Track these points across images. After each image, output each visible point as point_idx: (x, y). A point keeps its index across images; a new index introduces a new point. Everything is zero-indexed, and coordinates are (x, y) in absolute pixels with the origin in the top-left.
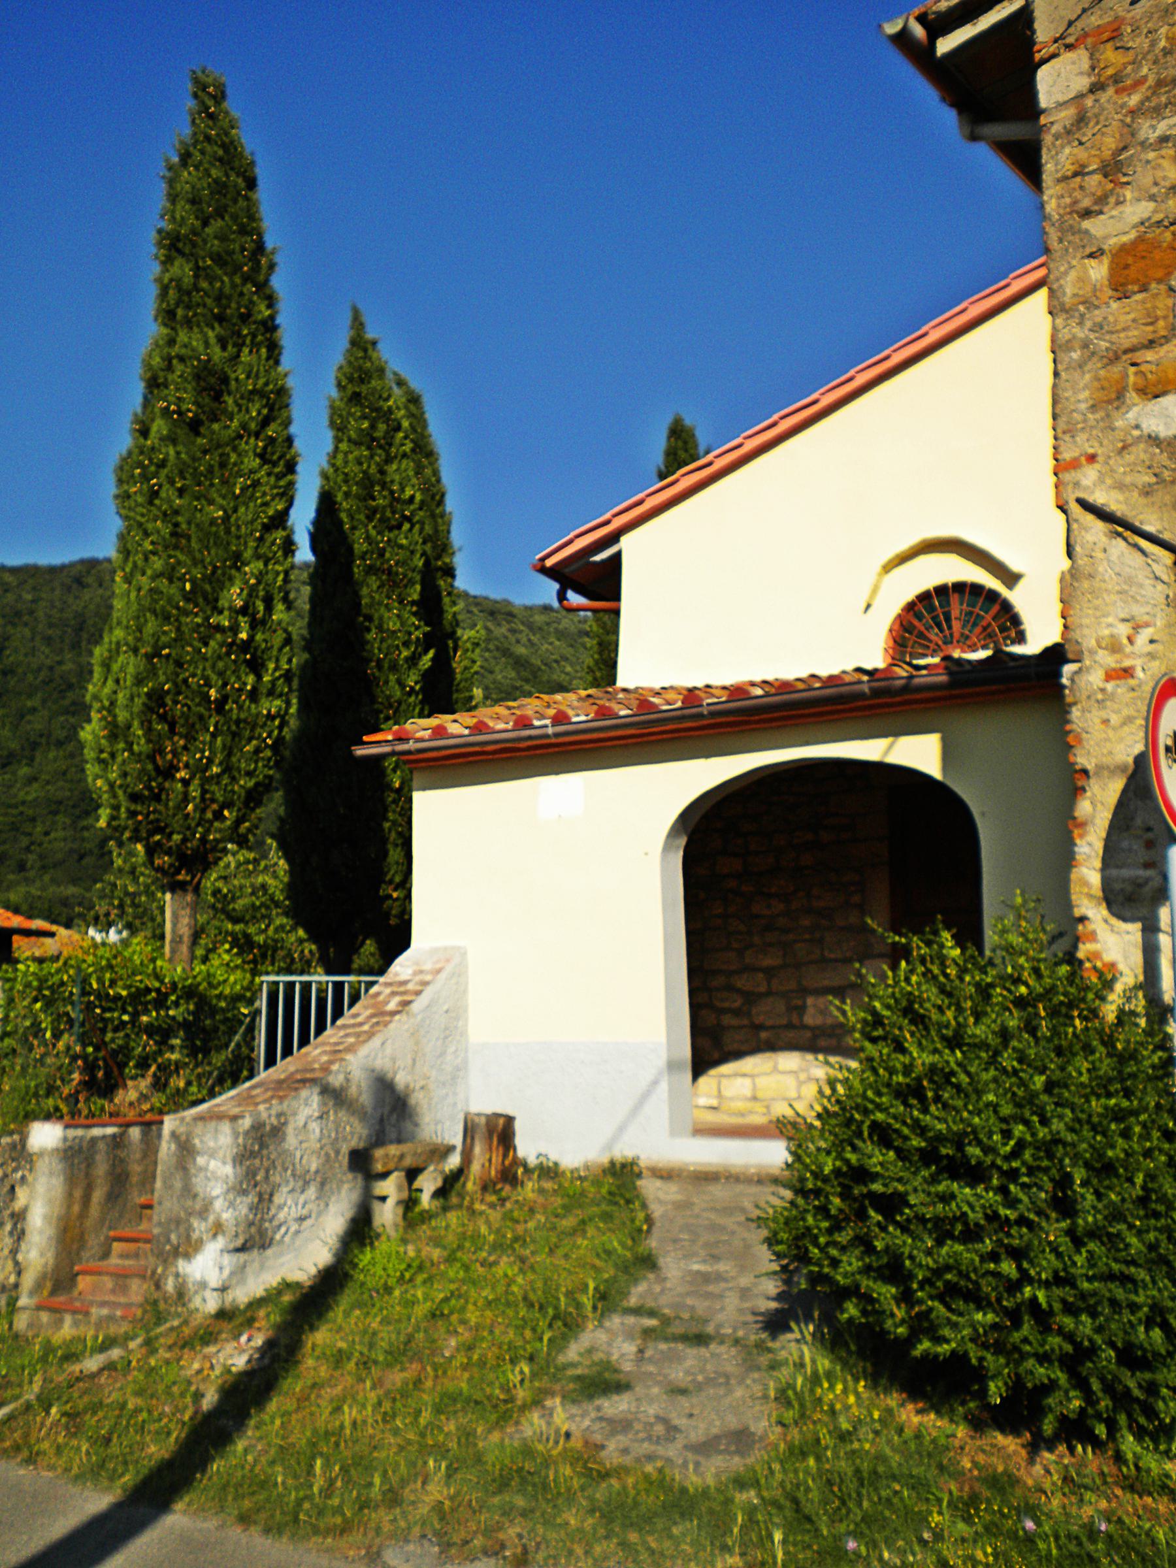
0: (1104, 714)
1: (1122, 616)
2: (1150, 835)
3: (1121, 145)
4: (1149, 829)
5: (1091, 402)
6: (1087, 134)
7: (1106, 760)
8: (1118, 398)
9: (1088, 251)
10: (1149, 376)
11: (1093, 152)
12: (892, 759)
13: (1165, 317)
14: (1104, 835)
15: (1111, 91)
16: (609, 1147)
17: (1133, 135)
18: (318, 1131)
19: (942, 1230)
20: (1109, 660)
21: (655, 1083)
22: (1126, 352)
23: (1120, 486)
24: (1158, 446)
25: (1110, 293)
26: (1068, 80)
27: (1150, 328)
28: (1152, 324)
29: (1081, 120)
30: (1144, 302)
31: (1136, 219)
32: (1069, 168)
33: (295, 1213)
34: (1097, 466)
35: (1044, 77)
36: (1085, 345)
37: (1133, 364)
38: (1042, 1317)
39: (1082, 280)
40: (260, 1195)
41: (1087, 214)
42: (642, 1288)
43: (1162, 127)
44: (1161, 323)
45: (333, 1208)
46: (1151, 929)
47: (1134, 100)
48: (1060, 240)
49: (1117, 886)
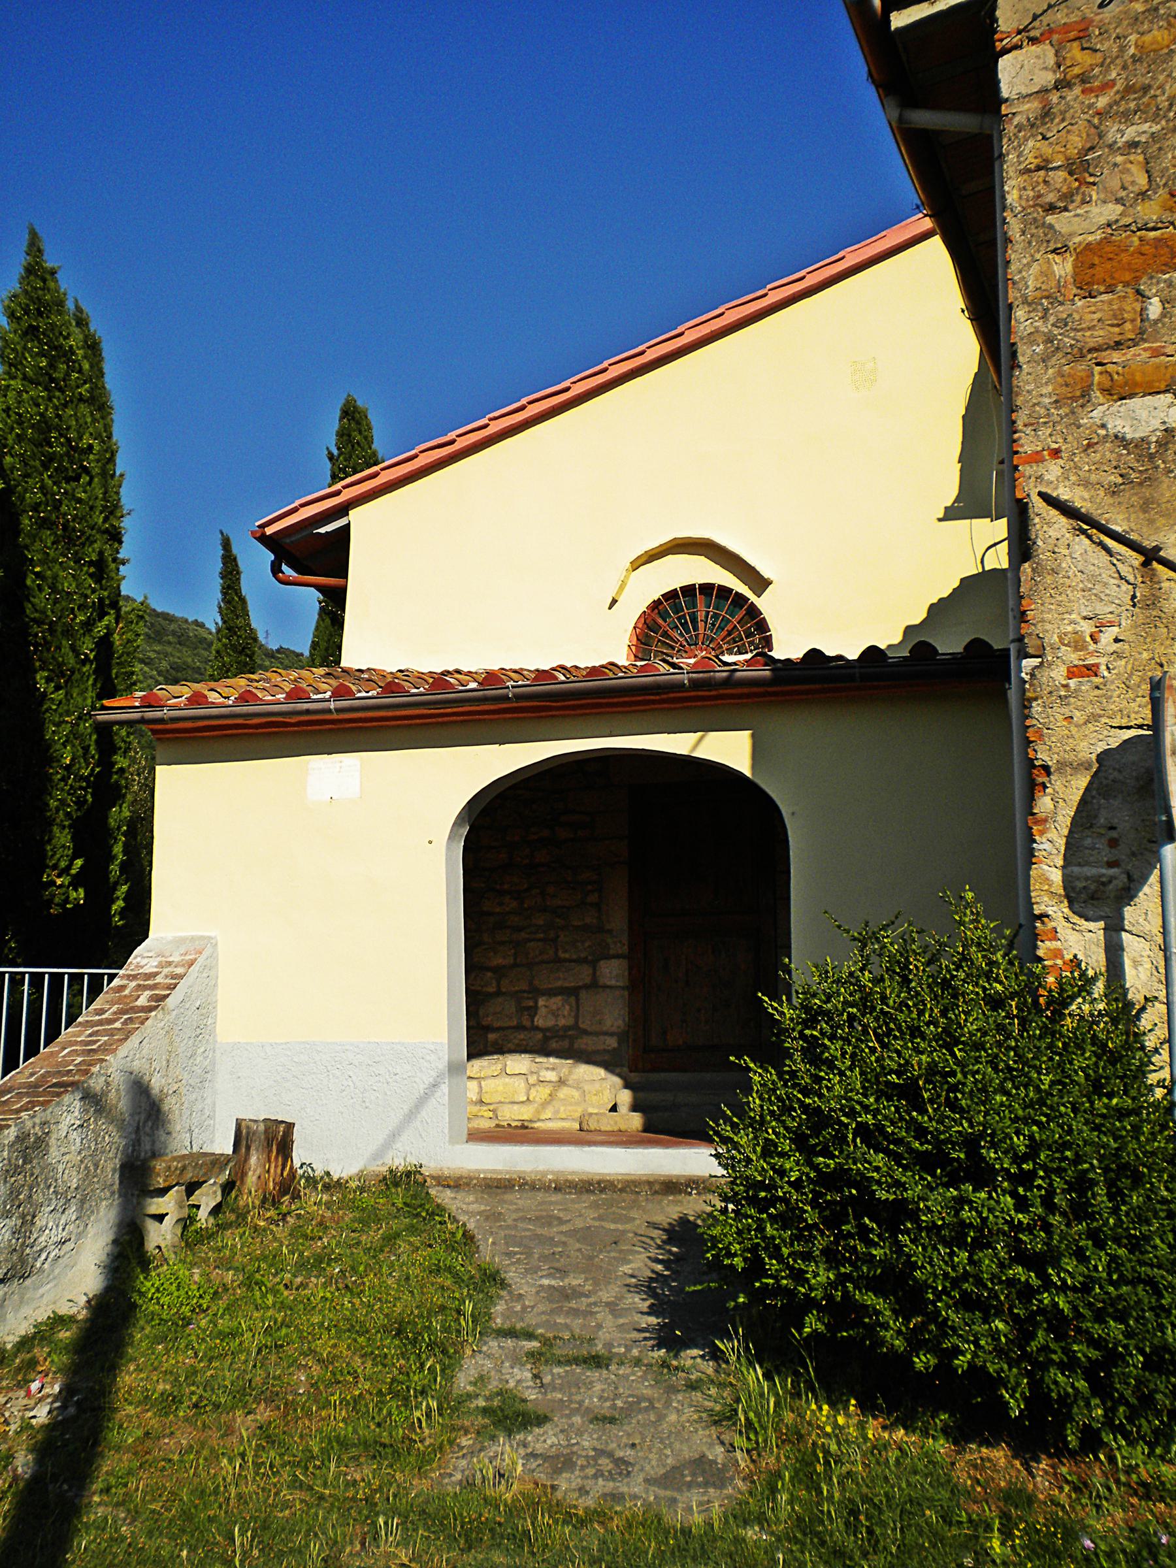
0: (1066, 711)
1: (1085, 614)
2: (1114, 834)
3: (1088, 145)
4: (1112, 828)
5: (1054, 398)
6: (1052, 131)
7: (1070, 757)
8: (1083, 396)
9: (1052, 246)
10: (1116, 377)
11: (1058, 148)
12: (701, 753)
13: (1133, 321)
14: (1066, 832)
15: (1077, 90)
16: (378, 1155)
17: (1100, 136)
18: (78, 1140)
19: (957, 1235)
20: (1073, 657)
21: (435, 1085)
22: (1090, 351)
23: (1086, 484)
24: (1125, 448)
25: (1075, 291)
26: (1031, 72)
27: (1117, 330)
28: (1118, 325)
29: (1046, 114)
30: (1110, 302)
31: (1103, 220)
32: (1031, 161)
33: (57, 1235)
34: (1060, 462)
35: (1006, 66)
36: (1049, 340)
37: (1098, 364)
38: (1057, 1323)
39: (1047, 274)
40: (23, 1216)
41: (1051, 208)
42: (499, 1307)
43: (1131, 133)
44: (1128, 326)
45: (91, 1230)
46: (1115, 927)
47: (1102, 102)
48: (1023, 233)
49: (1080, 885)
